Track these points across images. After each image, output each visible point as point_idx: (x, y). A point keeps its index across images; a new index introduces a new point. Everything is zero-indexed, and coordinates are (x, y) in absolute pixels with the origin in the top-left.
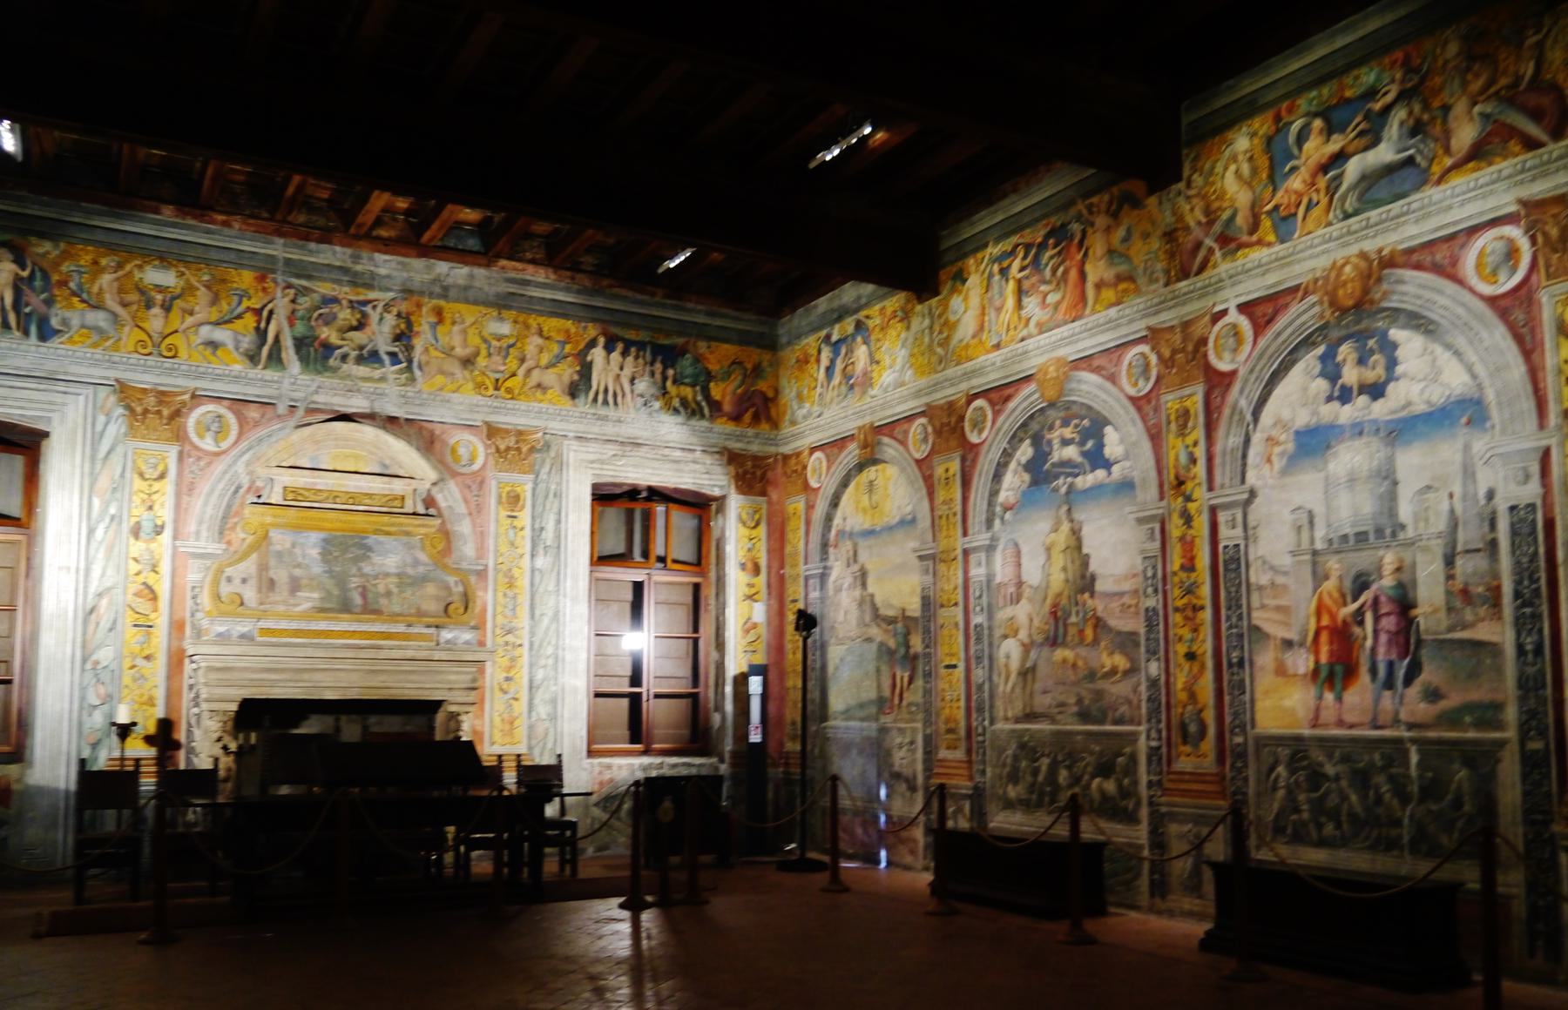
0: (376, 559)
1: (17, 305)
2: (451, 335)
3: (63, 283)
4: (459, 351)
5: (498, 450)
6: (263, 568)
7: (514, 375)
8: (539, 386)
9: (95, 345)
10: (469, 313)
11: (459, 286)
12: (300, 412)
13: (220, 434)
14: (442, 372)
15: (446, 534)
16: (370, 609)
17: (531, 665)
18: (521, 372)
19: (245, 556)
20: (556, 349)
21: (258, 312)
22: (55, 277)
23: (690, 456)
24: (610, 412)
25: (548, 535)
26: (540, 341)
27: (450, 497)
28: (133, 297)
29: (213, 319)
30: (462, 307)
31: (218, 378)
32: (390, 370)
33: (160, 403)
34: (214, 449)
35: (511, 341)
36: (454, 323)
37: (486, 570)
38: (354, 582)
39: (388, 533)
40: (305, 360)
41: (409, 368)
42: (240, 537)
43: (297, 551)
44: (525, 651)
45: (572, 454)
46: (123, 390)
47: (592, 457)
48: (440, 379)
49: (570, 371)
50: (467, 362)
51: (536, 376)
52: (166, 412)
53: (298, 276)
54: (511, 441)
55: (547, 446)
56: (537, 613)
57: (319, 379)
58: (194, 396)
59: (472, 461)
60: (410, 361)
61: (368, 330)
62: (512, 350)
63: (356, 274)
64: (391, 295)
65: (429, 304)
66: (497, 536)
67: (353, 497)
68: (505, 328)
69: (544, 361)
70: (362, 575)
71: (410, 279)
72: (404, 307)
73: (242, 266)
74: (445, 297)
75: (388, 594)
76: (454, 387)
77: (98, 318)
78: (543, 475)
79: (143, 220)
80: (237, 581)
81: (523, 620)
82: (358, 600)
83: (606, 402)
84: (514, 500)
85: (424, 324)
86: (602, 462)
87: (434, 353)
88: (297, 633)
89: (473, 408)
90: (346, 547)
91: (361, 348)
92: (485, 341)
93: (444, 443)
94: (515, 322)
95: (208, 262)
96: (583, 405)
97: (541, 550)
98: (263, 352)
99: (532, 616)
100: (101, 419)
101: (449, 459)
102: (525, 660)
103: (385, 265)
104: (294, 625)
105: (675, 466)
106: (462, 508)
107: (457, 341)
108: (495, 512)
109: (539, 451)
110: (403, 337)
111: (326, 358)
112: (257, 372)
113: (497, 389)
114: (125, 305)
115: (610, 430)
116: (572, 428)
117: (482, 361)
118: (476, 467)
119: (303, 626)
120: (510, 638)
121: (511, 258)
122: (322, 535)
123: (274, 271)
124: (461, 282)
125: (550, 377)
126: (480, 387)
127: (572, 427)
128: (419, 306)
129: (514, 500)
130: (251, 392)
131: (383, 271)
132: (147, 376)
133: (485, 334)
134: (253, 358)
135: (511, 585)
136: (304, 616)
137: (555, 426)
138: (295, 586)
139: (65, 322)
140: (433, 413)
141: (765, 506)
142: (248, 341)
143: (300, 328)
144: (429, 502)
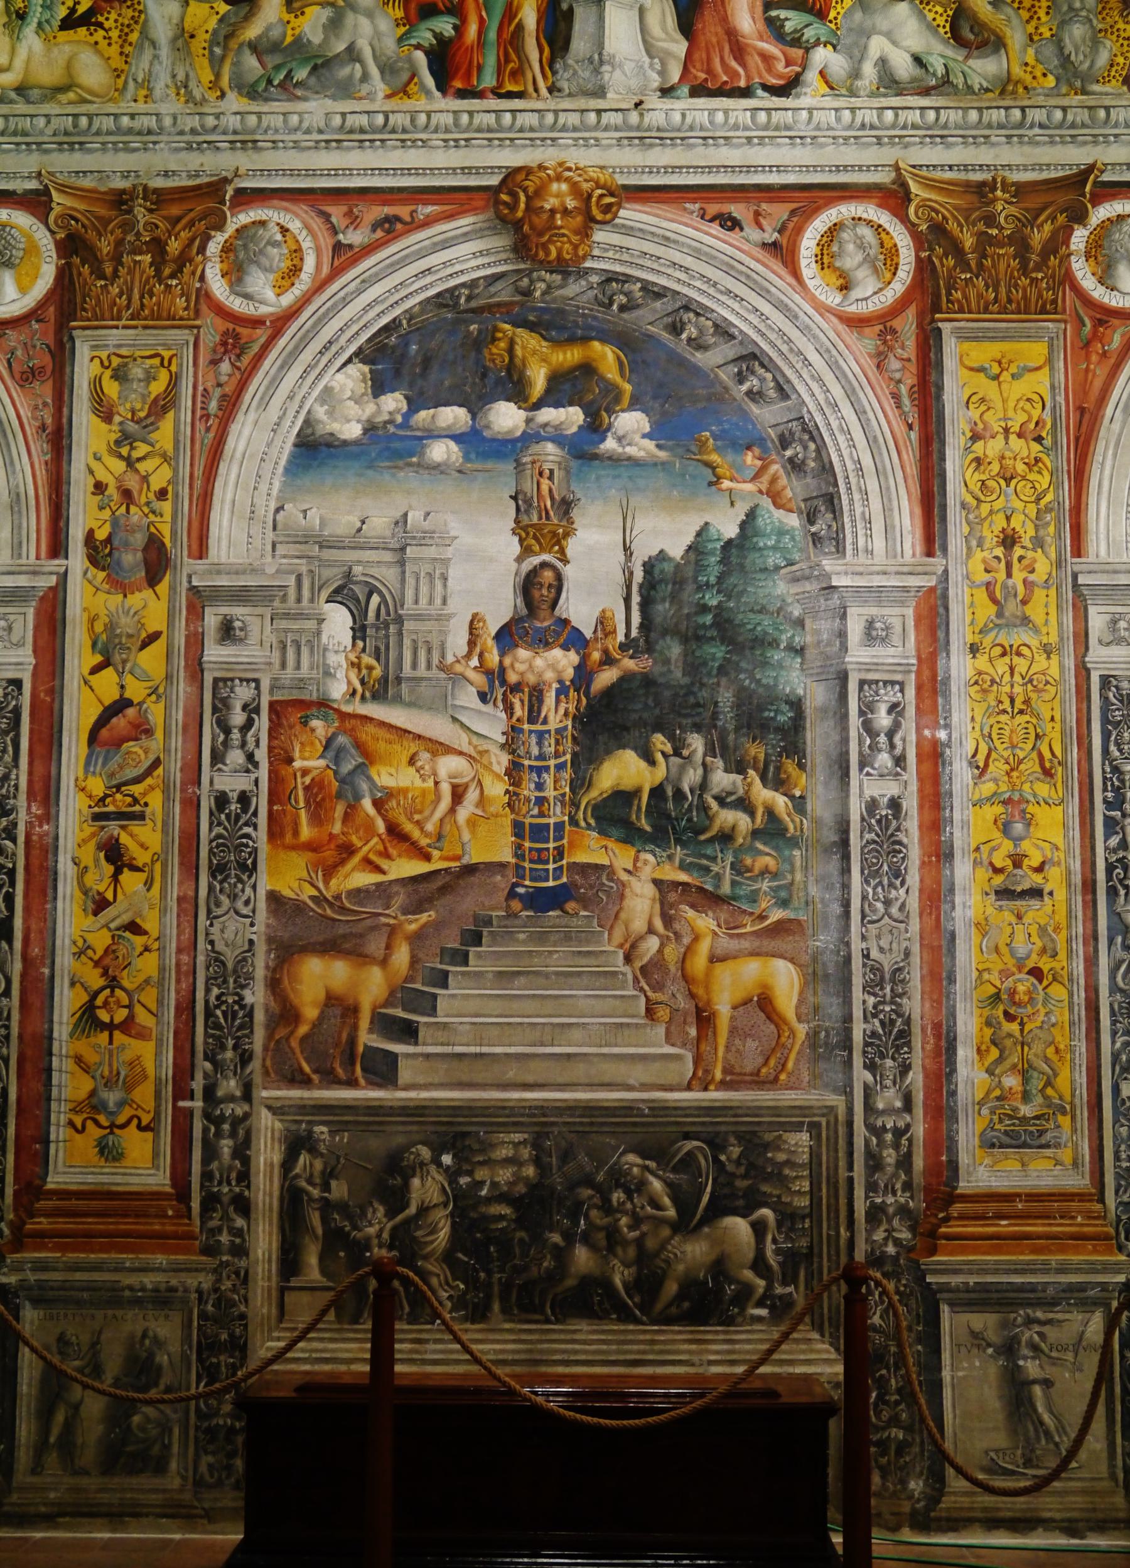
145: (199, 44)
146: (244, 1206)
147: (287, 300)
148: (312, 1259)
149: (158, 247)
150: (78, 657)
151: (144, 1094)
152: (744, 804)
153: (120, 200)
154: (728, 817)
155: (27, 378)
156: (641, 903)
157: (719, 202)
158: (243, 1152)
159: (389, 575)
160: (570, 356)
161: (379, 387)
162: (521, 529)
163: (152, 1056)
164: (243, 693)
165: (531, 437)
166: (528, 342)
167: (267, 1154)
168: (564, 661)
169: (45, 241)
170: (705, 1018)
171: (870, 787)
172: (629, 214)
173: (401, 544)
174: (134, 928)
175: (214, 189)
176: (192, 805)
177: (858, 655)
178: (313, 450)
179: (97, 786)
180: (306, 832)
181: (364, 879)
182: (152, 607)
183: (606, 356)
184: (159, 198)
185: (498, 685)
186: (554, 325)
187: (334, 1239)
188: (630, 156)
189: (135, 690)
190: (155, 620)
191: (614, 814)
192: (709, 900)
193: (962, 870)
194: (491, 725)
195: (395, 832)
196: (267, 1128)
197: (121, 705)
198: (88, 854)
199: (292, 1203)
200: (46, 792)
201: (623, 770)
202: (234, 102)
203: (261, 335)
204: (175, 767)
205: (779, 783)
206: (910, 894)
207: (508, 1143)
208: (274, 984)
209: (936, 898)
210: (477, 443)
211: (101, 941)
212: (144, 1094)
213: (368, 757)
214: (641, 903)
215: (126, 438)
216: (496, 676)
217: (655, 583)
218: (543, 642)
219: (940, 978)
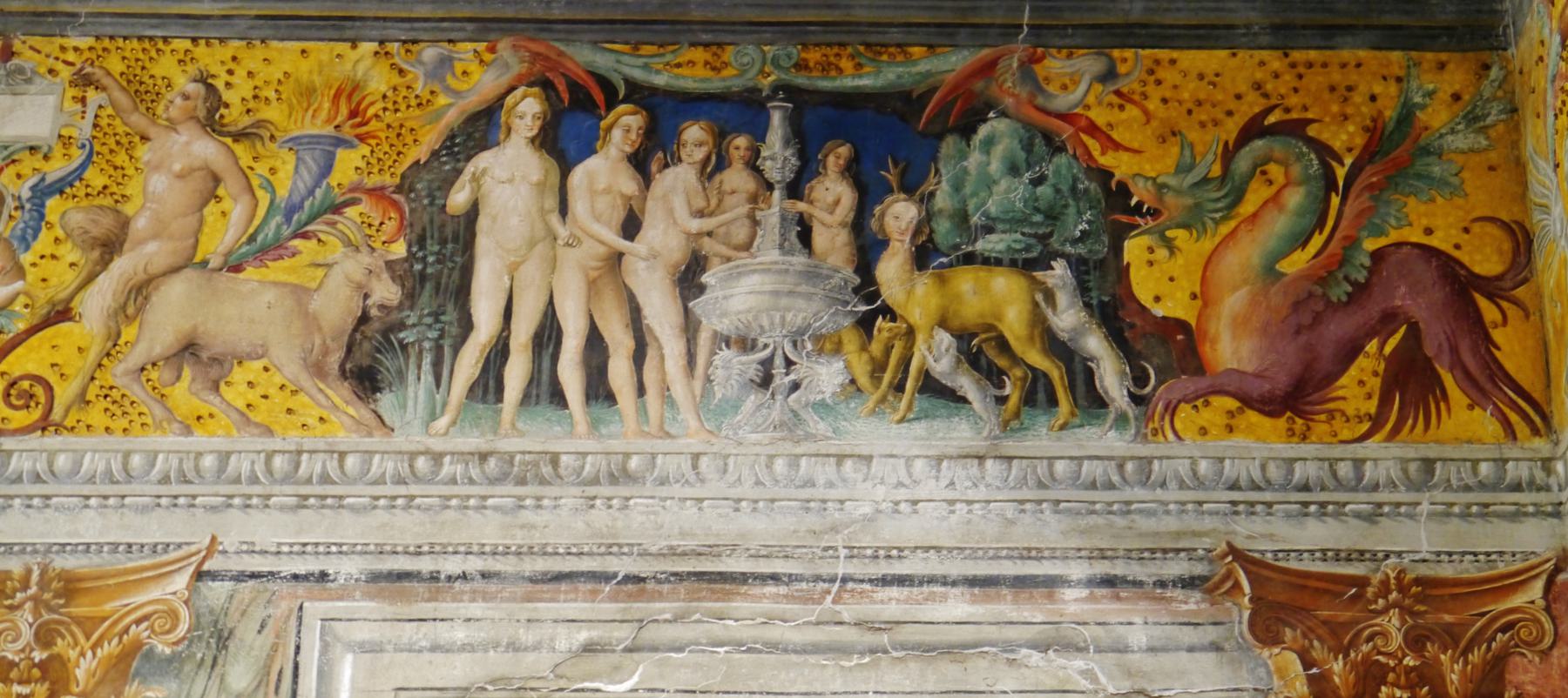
7: (61, 313)
8: (189, 349)
24: (572, 435)
26: (206, 149)
35: (56, 168)
49: (353, 266)
51: (173, 311)
55: (218, 638)
62: (53, 205)
83: (545, 391)
94: (84, 80)
96: (422, 415)
109: (170, 666)
125: (250, 309)
127: (350, 529)
137: (260, 533)
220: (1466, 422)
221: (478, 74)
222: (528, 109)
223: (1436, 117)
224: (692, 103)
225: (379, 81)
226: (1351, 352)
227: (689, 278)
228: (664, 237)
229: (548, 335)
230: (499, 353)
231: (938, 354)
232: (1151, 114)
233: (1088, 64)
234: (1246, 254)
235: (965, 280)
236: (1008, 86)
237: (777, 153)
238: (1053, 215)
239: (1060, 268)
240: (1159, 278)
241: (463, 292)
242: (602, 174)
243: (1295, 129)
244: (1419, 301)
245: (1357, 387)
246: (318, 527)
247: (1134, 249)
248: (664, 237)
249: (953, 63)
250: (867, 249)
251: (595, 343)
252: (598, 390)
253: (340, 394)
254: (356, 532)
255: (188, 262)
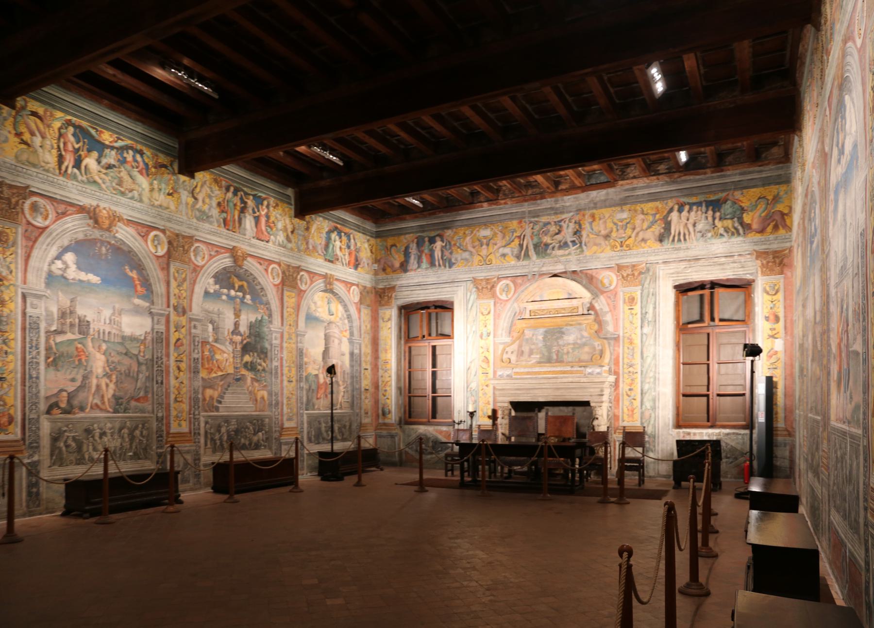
0: (566, 338)
1: (442, 258)
2: (600, 227)
3: (455, 245)
4: (603, 232)
5: (623, 277)
6: (520, 346)
7: (630, 237)
8: (643, 240)
9: (465, 266)
10: (606, 212)
11: (602, 201)
12: (537, 277)
13: (508, 292)
14: (596, 244)
15: (599, 322)
16: (559, 361)
17: (642, 383)
18: (633, 235)
19: (513, 342)
20: (651, 218)
21: (519, 237)
22: (453, 243)
23: (731, 259)
24: (683, 245)
25: (650, 316)
26: (642, 216)
27: (601, 304)
28: (477, 243)
29: (504, 244)
30: (603, 210)
31: (506, 268)
32: (572, 249)
33: (487, 283)
34: (506, 298)
36: (600, 219)
37: (619, 336)
38: (555, 349)
39: (571, 325)
40: (537, 253)
41: (581, 246)
42: (515, 335)
43: (534, 338)
44: (639, 375)
45: (661, 272)
46: (475, 281)
47: (672, 271)
48: (595, 248)
49: (659, 228)
50: (607, 237)
52: (489, 287)
53: (534, 217)
54: (629, 271)
55: (648, 270)
56: (645, 356)
57: (544, 260)
58: (498, 278)
59: (610, 285)
60: (581, 243)
61: (562, 233)
63: (557, 209)
64: (572, 214)
65: (588, 213)
66: (624, 319)
67: (557, 311)
68: (625, 215)
69: (645, 227)
70: (559, 345)
71: (579, 204)
72: (577, 218)
73: (513, 219)
74: (595, 208)
75: (568, 353)
76: (600, 250)
77: (466, 255)
78: (646, 285)
79: (479, 212)
80: (510, 353)
81: (637, 360)
82: (555, 357)
83: (679, 240)
84: (632, 300)
85: (586, 226)
86: (678, 273)
87: (591, 236)
88: (528, 373)
89: (610, 259)
90: (554, 333)
91: (560, 242)
92: (615, 224)
93: (597, 279)
95: (500, 221)
96: (667, 244)
97: (646, 324)
98: (522, 254)
99: (642, 358)
100: (469, 294)
101: (600, 285)
102: (639, 380)
103: (569, 201)
104: (526, 370)
105: (722, 267)
106: (606, 309)
107: (602, 228)
108: (622, 307)
110: (577, 233)
111: (546, 250)
112: (522, 263)
113: (621, 246)
114: (474, 247)
115: (682, 254)
116: (660, 258)
117: (614, 235)
118: (612, 288)
119: (530, 370)
120: (631, 369)
121: (623, 179)
122: (544, 330)
123: (524, 218)
124: (603, 198)
125: (649, 234)
126: (613, 247)
128: (584, 215)
129: (632, 300)
130: (519, 272)
131: (568, 204)
132: (481, 275)
133: (615, 221)
134: (518, 257)
135: (631, 343)
136: (532, 366)
137: (652, 259)
138: (531, 353)
139: (456, 260)
140: (592, 265)
141: (782, 280)
142: (516, 251)
143: (536, 240)
144: (591, 308)
145: (189, 206)
146: (199, 434)
147: (203, 263)
148: (209, 442)
149: (183, 247)
150: (172, 329)
151: (184, 414)
152: (260, 365)
153: (177, 235)
154: (259, 367)
155: (163, 269)
156: (249, 381)
157: (260, 260)
158: (199, 425)
159: (217, 319)
160: (240, 283)
161: (216, 284)
162: (235, 314)
163: (185, 407)
164: (197, 339)
165: (236, 297)
166: (236, 280)
167: (202, 425)
168: (238, 338)
169: (165, 240)
170: (256, 400)
171: (275, 363)
172: (249, 259)
173: (219, 314)
174: (182, 383)
175: (191, 237)
176: (190, 359)
177: (274, 342)
178: (207, 293)
179: (176, 355)
180: (207, 366)
181: (214, 375)
182: (183, 320)
183: (245, 284)
184: (184, 237)
185: (232, 342)
186: (239, 277)
187: (212, 439)
188: (248, 248)
189: (181, 337)
190: (184, 324)
191: (246, 365)
192: (257, 381)
193: (285, 378)
194: (230, 348)
195: (219, 367)
196: (202, 420)
197: (178, 340)
198: (175, 368)
199: (206, 432)
200: (168, 355)
201: (247, 358)
202: (195, 220)
203: (199, 269)
204: (187, 351)
205: (265, 362)
206: (279, 381)
207: (234, 422)
208: (203, 394)
209: (282, 381)
210: (228, 295)
211: (177, 385)
212: (184, 414)
213: (215, 353)
214: (249, 381)
215: (179, 286)
216: (231, 339)
217: (251, 326)
218: (237, 334)
219: (282, 394)
220: (782, 231)
221: (670, 203)
222: (676, 207)
223: (781, 193)
224: (694, 204)
225: (660, 206)
226: (769, 225)
227: (694, 225)
228: (691, 221)
229: (679, 234)
230: (674, 237)
231: (722, 231)
232: (746, 198)
233: (740, 192)
234: (757, 214)
235: (725, 222)
236: (730, 197)
237: (704, 208)
238: (735, 212)
239: (736, 219)
240: (747, 218)
241: (670, 230)
242: (685, 213)
243: (764, 197)
244: (777, 217)
245: (769, 229)
246: (657, 258)
247: (744, 215)
248: (691, 221)
249: (723, 195)
250: (714, 219)
251: (685, 235)
252: (685, 239)
253: (658, 243)
254: (660, 258)
255: (642, 230)
